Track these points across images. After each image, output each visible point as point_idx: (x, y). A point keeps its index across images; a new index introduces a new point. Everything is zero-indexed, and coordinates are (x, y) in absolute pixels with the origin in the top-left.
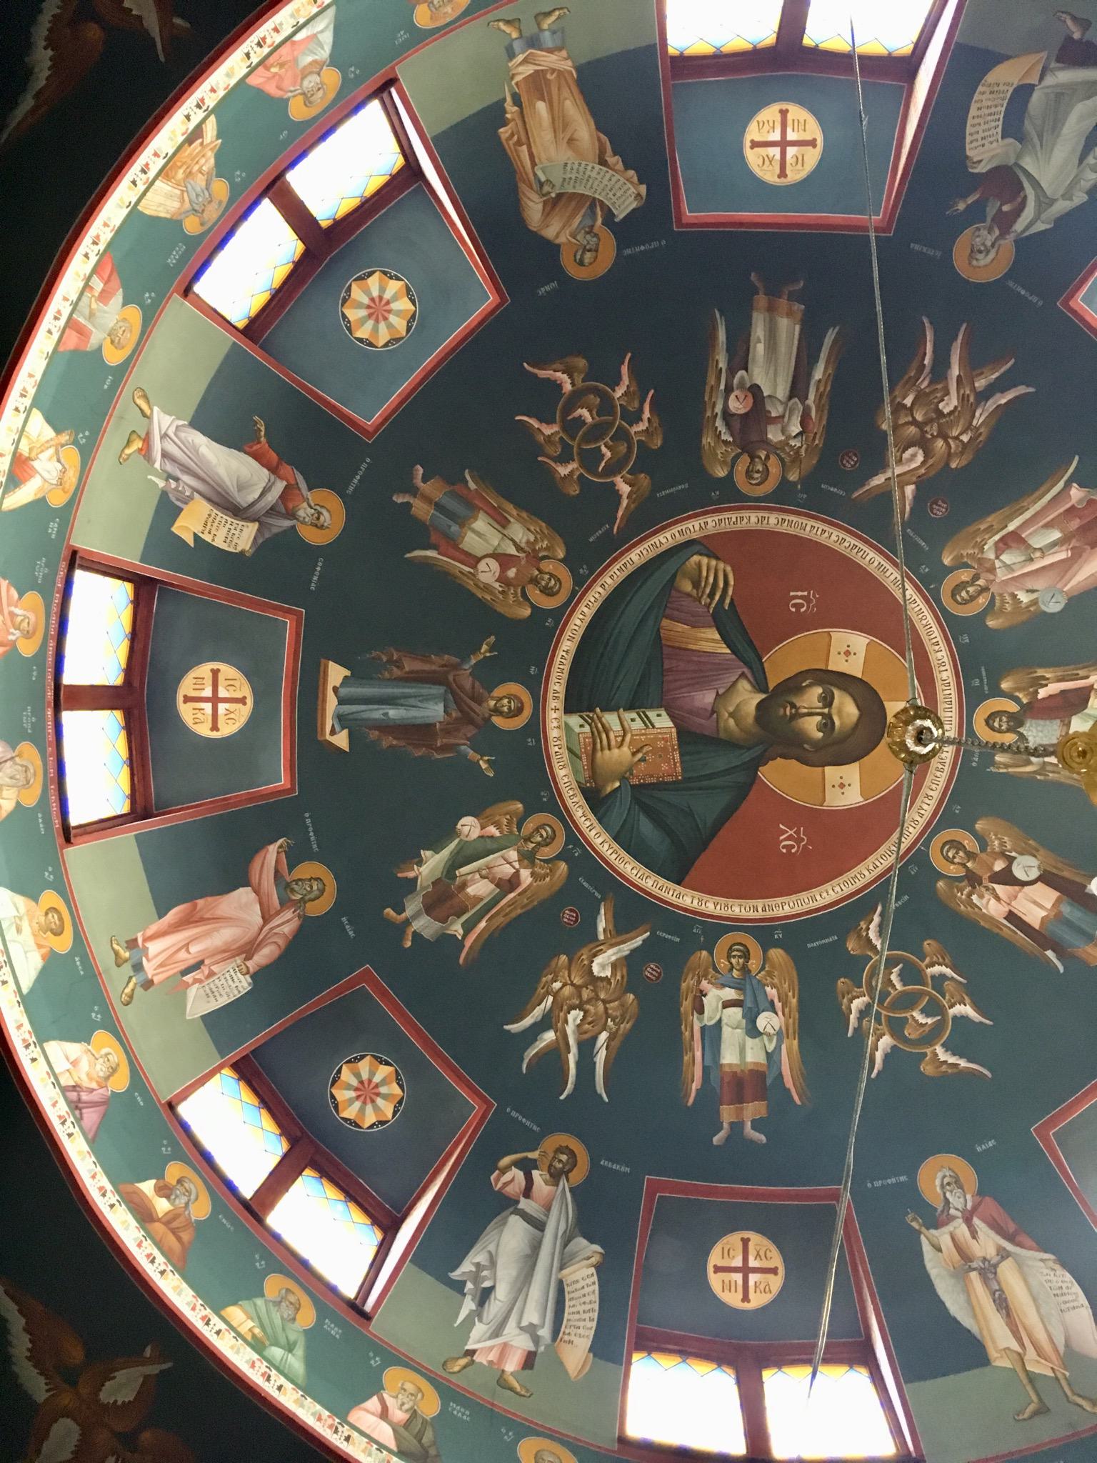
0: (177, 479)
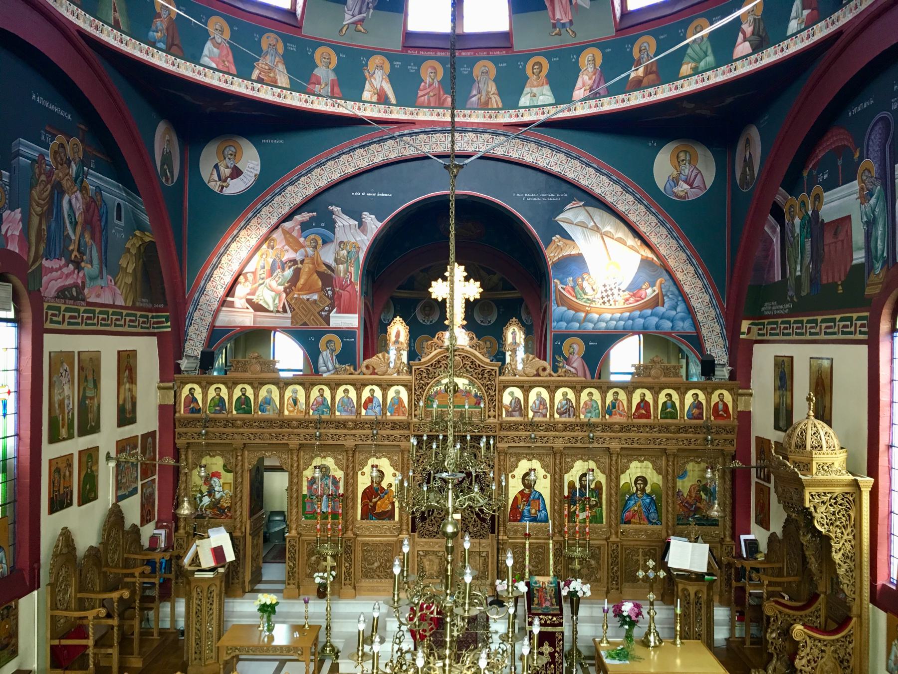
0: (368, 4)
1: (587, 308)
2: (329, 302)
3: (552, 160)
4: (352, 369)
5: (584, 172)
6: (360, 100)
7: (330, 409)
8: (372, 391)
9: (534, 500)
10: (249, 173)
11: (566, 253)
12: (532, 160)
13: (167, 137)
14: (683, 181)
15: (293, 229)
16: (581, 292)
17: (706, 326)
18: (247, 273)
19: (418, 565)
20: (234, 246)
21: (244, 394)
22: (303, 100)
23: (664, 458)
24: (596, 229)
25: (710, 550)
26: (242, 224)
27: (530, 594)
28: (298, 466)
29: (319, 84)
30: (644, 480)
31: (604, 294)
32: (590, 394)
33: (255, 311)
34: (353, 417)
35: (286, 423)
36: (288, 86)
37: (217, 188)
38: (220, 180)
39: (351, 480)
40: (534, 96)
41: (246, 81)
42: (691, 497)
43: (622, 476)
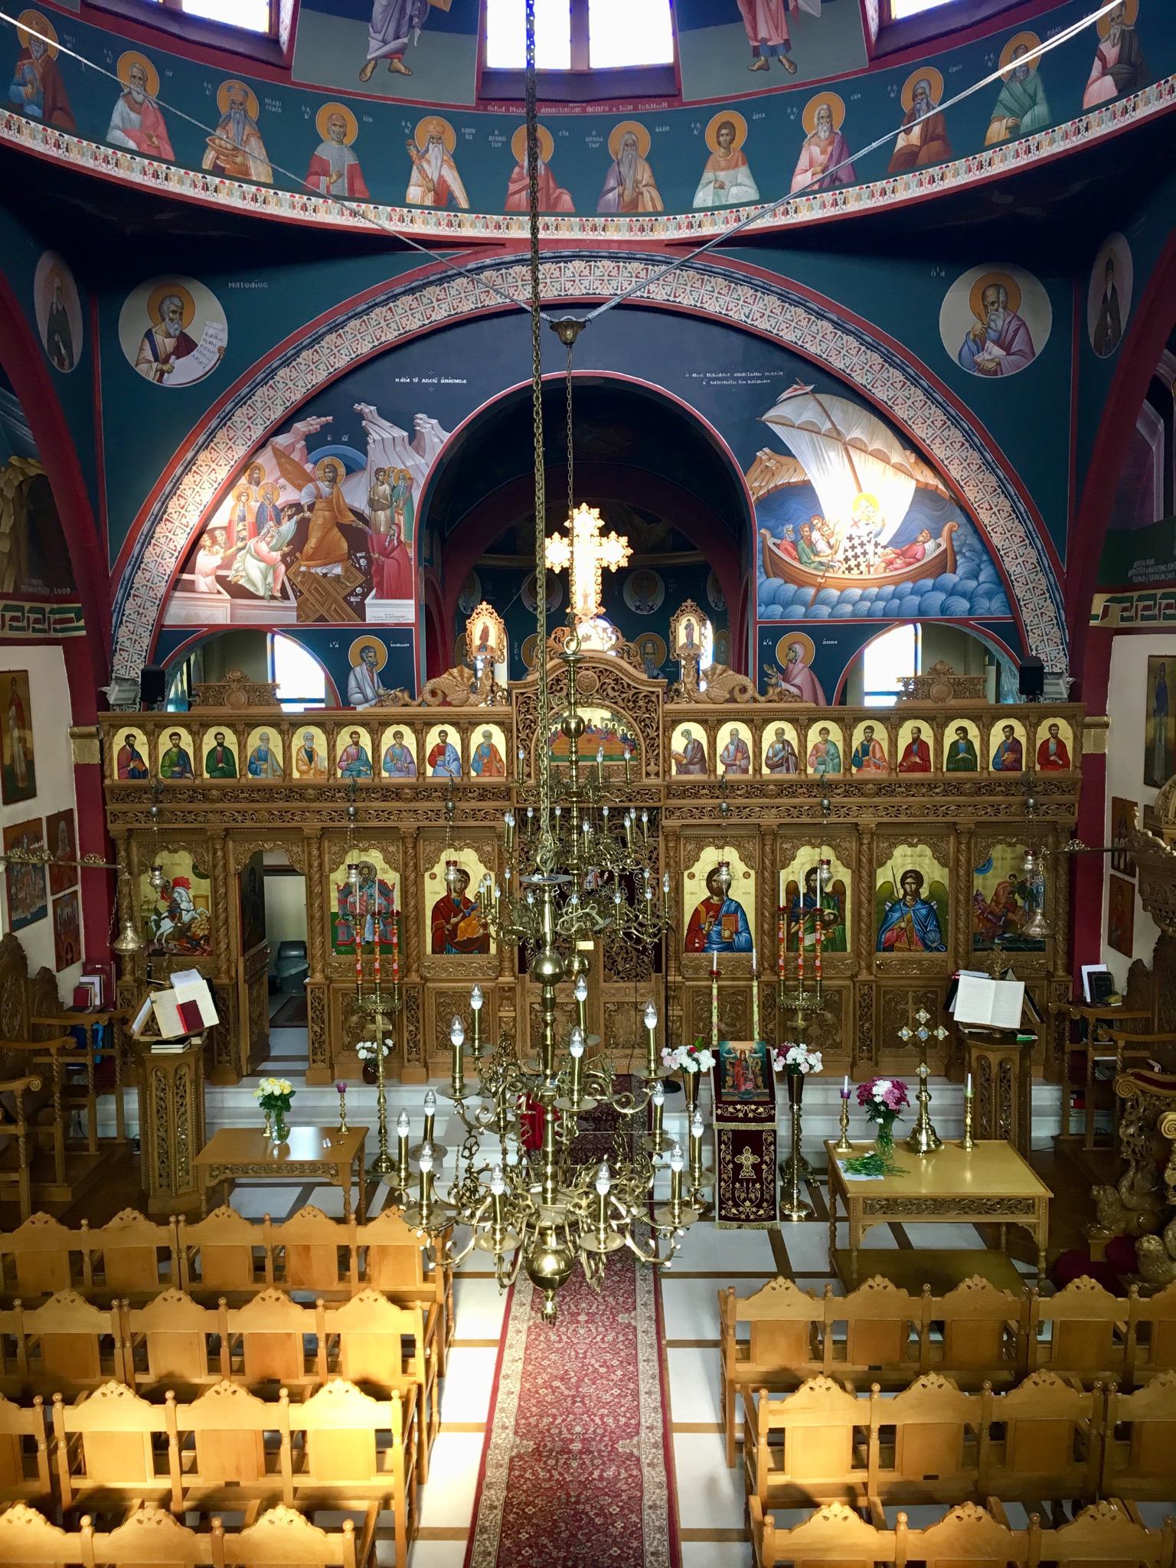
0: (411, 18)
1: (819, 580)
2: (361, 579)
3: (755, 308)
4: (406, 696)
5: (814, 329)
6: (403, 203)
7: (372, 767)
8: (443, 734)
9: (727, 914)
10: (209, 346)
11: (780, 481)
12: (718, 309)
13: (57, 283)
14: (994, 342)
15: (292, 447)
16: (808, 550)
17: (1031, 606)
18: (215, 529)
19: (532, 1026)
20: (188, 480)
21: (220, 744)
22: (298, 206)
23: (952, 839)
24: (834, 435)
25: (1026, 991)
26: (201, 439)
27: (719, 1071)
28: (321, 865)
29: (326, 174)
30: (918, 877)
31: (850, 554)
32: (825, 731)
33: (233, 597)
34: (412, 780)
35: (296, 792)
36: (270, 181)
37: (152, 374)
38: (156, 359)
39: (412, 888)
40: (722, 187)
41: (192, 174)
42: (997, 903)
43: (879, 871)
